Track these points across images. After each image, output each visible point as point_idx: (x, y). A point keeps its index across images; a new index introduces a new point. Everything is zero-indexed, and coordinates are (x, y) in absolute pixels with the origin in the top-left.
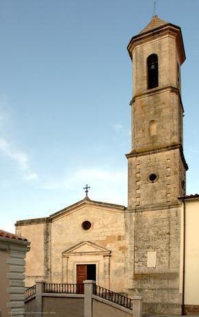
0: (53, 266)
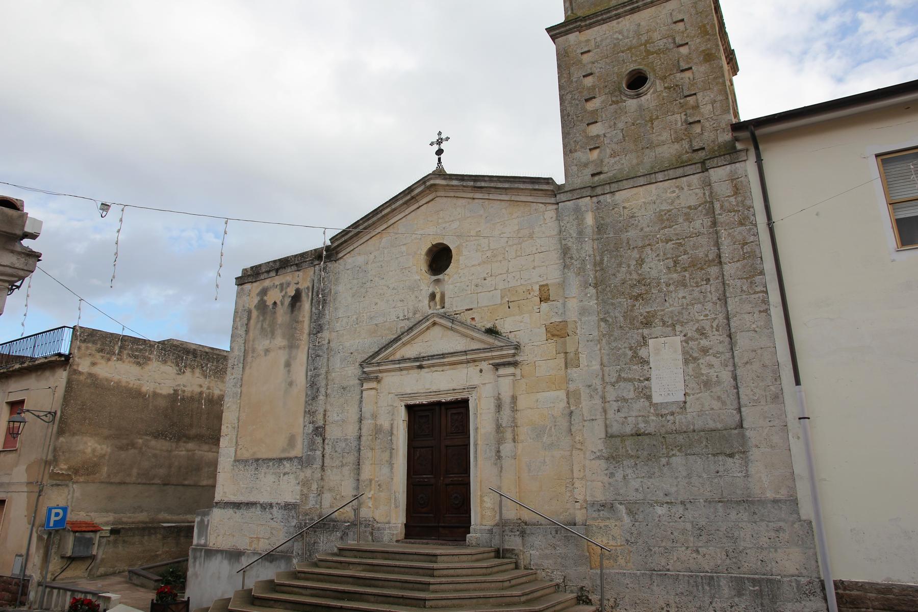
0: (333, 416)
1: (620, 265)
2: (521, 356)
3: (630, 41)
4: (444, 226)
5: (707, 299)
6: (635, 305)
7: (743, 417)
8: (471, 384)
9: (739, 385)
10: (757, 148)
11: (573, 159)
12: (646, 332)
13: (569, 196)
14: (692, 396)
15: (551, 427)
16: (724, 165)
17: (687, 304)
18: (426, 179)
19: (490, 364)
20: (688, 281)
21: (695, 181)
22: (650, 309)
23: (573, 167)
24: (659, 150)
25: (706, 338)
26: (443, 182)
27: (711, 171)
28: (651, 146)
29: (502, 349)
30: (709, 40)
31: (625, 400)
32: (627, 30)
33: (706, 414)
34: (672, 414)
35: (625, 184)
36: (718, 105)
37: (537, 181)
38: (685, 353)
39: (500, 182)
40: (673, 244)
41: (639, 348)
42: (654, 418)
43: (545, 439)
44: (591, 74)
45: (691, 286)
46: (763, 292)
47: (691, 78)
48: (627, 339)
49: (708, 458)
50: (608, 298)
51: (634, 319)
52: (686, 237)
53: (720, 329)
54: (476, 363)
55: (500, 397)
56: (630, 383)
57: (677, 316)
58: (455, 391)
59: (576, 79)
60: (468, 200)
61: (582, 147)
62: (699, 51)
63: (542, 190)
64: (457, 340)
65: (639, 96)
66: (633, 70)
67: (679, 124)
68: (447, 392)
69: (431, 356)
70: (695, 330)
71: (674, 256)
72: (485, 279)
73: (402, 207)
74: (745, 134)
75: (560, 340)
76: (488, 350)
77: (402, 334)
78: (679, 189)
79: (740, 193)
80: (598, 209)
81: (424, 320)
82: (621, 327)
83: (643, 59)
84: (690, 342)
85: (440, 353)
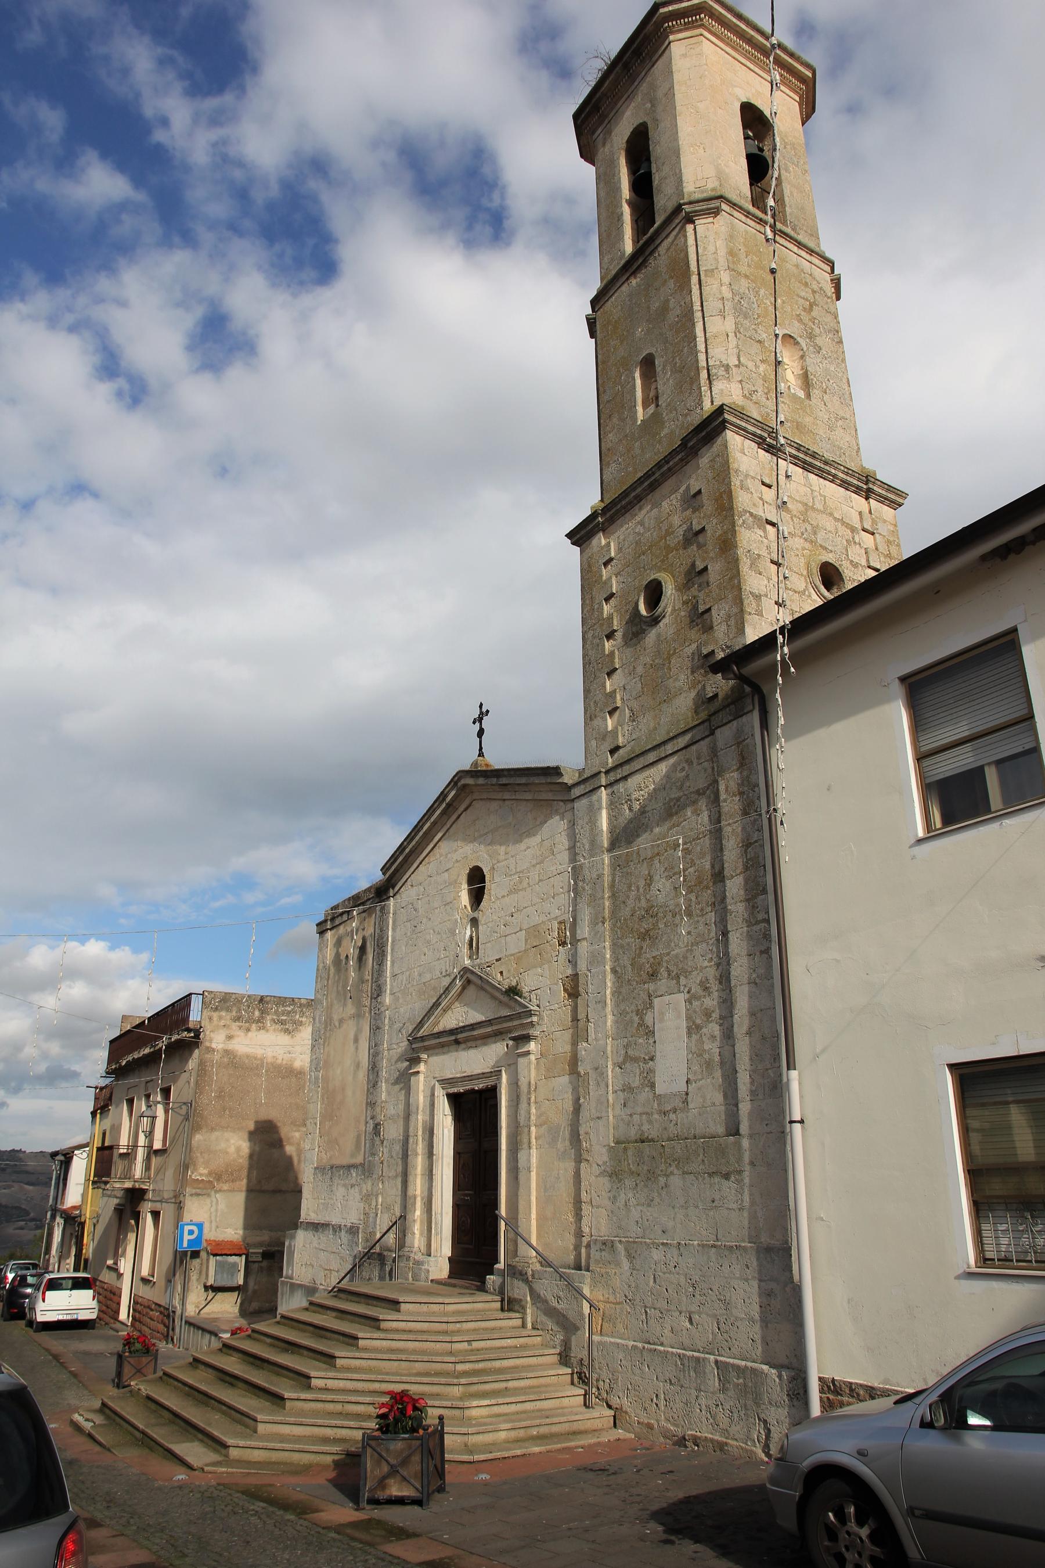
1: (629, 887)
12: (651, 987)
22: (657, 953)
34: (675, 1110)
42: (656, 1116)
49: (704, 1179)
77: (440, 997)
83: (663, 561)
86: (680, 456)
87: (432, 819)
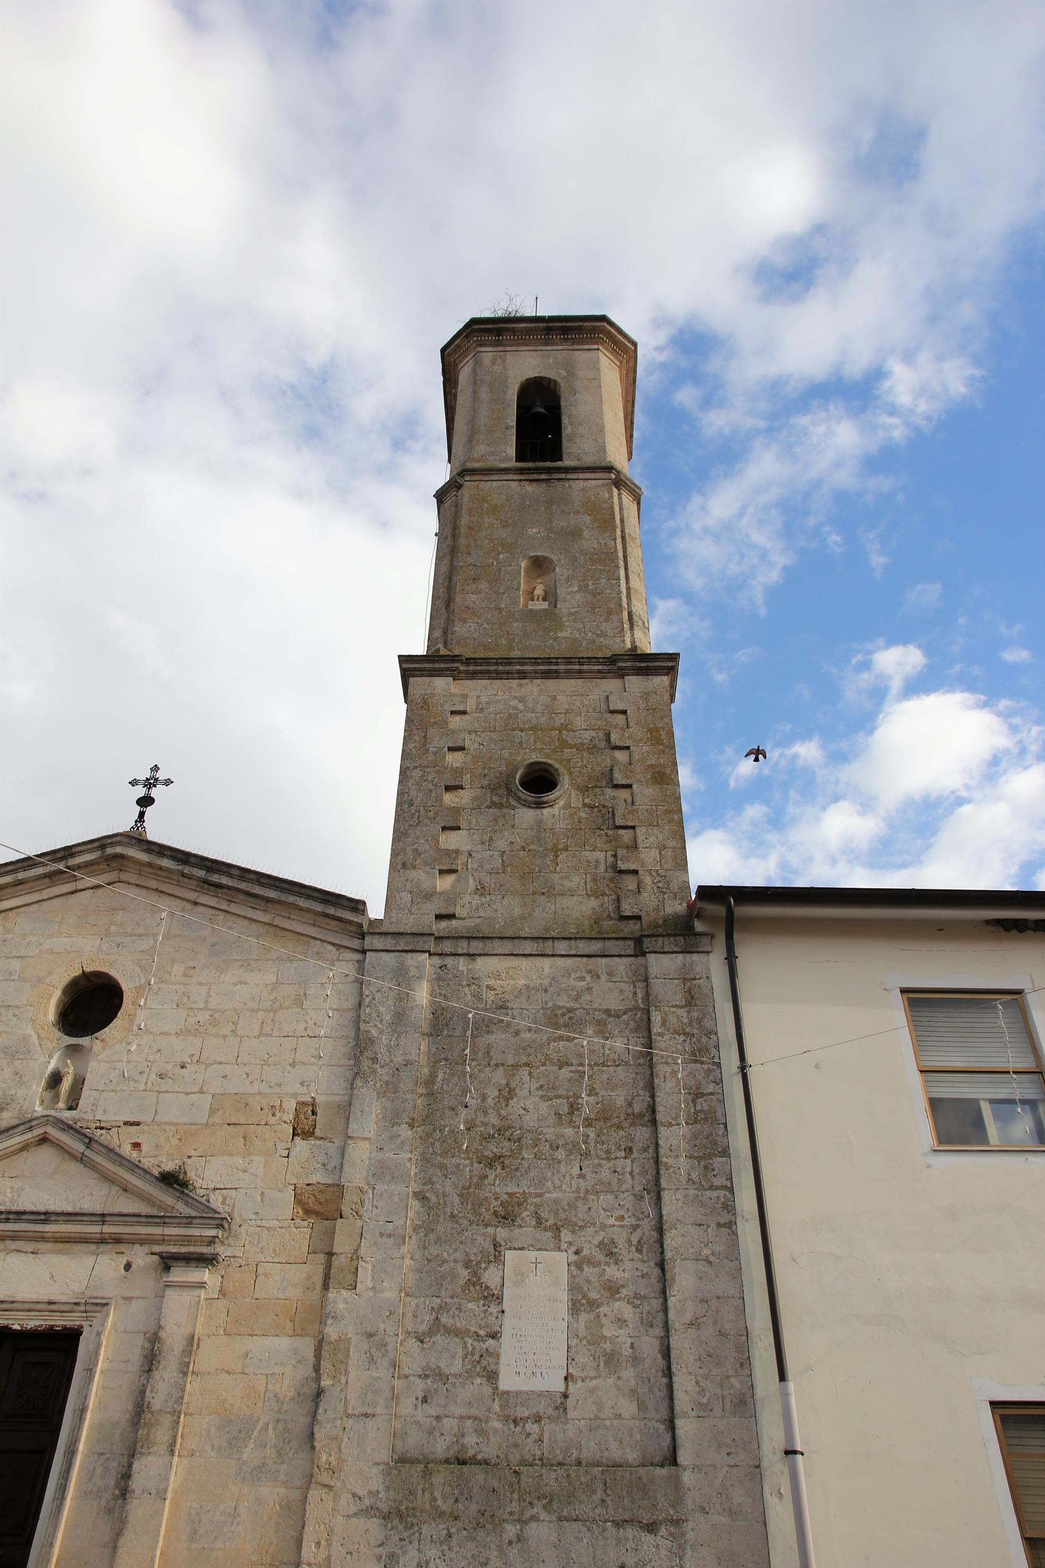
2: (229, 1245)
3: (537, 718)
4: (119, 939)
5: (625, 1187)
6: (487, 1176)
7: (679, 1441)
8: (95, 1294)
9: (674, 1369)
10: (729, 937)
11: (407, 880)
12: (502, 1233)
13: (389, 943)
14: (579, 1383)
15: (267, 1424)
16: (673, 952)
17: (587, 1191)
18: (109, 841)
19: (152, 1254)
20: (592, 1145)
21: (621, 968)
22: (516, 1190)
23: (403, 894)
24: (563, 902)
25: (616, 1263)
26: (143, 857)
27: (651, 958)
28: (550, 892)
29: (190, 1223)
30: (663, 753)
31: (442, 1377)
32: (533, 699)
33: (605, 1426)
34: (538, 1419)
35: (498, 946)
36: (669, 853)
37: (334, 900)
38: (574, 1288)
39: (261, 884)
40: (571, 1072)
41: (483, 1266)
42: (496, 1424)
43: (247, 1453)
44: (462, 749)
45: (598, 1157)
46: (725, 1188)
47: (629, 801)
48: (461, 1243)
50: (434, 1153)
51: (481, 1205)
52: (596, 1064)
53: (644, 1250)
54: (122, 1247)
55: (162, 1334)
56: (458, 1340)
57: (565, 1211)
58: (53, 1307)
59: (434, 749)
60: (185, 903)
61: (426, 864)
62: (647, 764)
63: (339, 919)
64: (87, 1186)
65: (539, 805)
66: (536, 763)
67: (602, 868)
68: (31, 1306)
69: (17, 1213)
70: (596, 1243)
71: (571, 1093)
72: (182, 1067)
73: (39, 882)
74: (719, 910)
75: (322, 1225)
76: (157, 1220)
78: (592, 976)
79: (696, 1005)
80: (439, 978)
81: (22, 1128)
82: (452, 1216)
83: (554, 751)
84: (586, 1268)
85: (41, 1208)
86: (600, 667)
87: (21, 876)
